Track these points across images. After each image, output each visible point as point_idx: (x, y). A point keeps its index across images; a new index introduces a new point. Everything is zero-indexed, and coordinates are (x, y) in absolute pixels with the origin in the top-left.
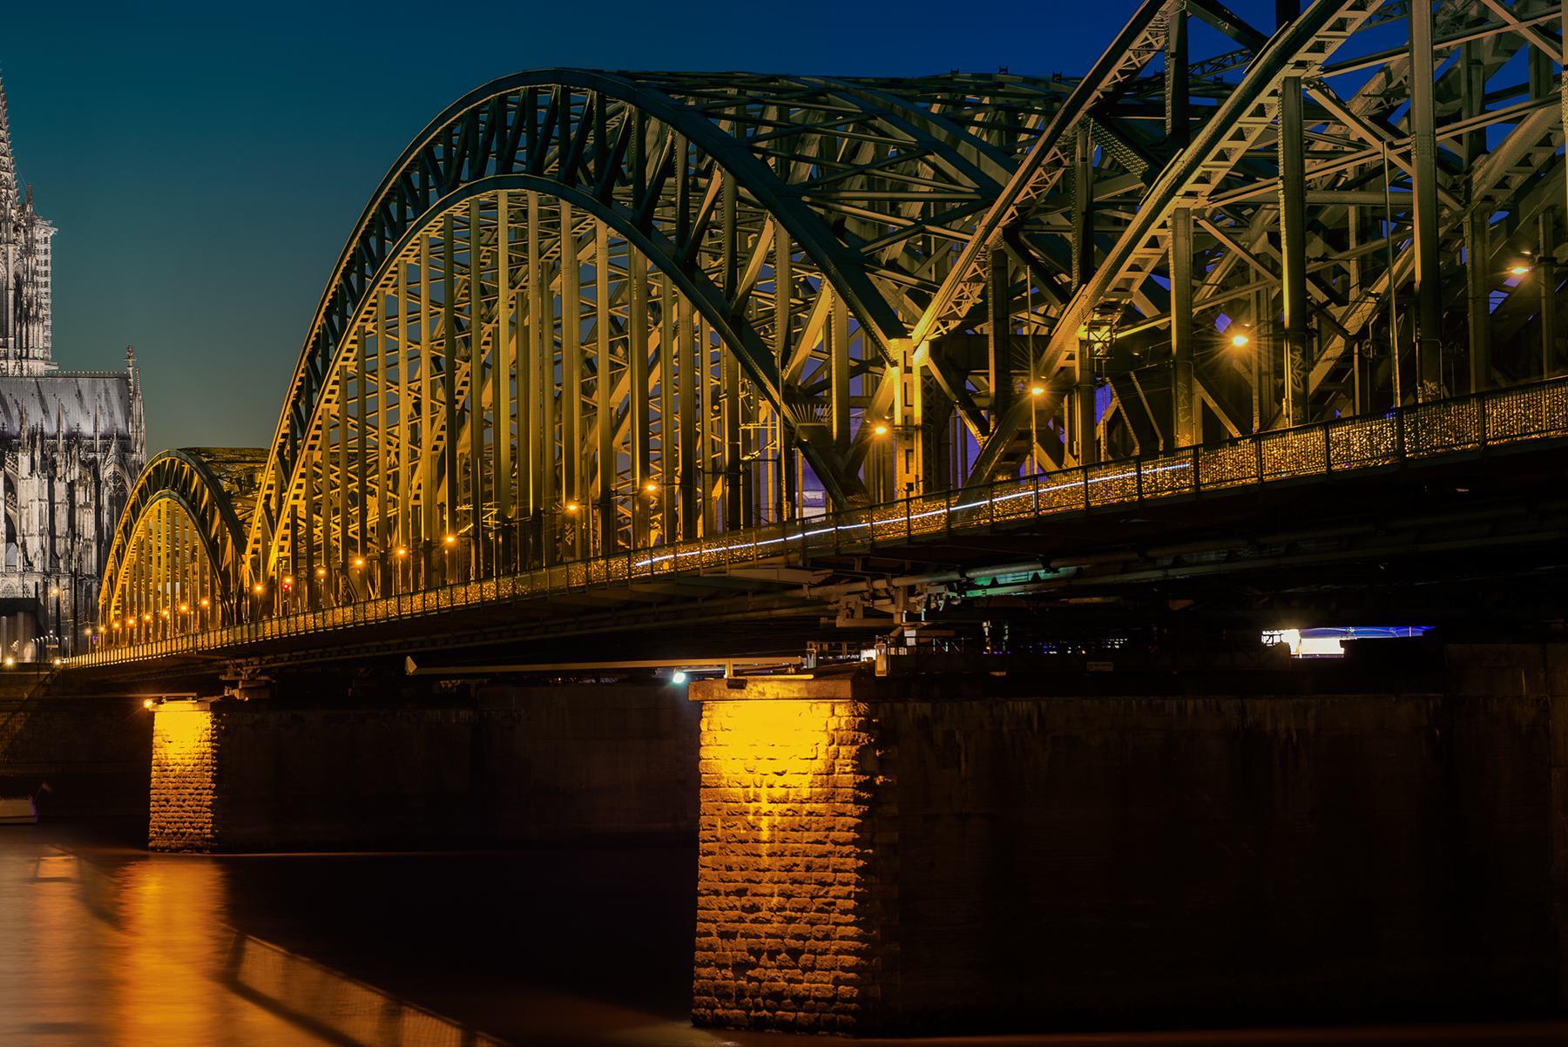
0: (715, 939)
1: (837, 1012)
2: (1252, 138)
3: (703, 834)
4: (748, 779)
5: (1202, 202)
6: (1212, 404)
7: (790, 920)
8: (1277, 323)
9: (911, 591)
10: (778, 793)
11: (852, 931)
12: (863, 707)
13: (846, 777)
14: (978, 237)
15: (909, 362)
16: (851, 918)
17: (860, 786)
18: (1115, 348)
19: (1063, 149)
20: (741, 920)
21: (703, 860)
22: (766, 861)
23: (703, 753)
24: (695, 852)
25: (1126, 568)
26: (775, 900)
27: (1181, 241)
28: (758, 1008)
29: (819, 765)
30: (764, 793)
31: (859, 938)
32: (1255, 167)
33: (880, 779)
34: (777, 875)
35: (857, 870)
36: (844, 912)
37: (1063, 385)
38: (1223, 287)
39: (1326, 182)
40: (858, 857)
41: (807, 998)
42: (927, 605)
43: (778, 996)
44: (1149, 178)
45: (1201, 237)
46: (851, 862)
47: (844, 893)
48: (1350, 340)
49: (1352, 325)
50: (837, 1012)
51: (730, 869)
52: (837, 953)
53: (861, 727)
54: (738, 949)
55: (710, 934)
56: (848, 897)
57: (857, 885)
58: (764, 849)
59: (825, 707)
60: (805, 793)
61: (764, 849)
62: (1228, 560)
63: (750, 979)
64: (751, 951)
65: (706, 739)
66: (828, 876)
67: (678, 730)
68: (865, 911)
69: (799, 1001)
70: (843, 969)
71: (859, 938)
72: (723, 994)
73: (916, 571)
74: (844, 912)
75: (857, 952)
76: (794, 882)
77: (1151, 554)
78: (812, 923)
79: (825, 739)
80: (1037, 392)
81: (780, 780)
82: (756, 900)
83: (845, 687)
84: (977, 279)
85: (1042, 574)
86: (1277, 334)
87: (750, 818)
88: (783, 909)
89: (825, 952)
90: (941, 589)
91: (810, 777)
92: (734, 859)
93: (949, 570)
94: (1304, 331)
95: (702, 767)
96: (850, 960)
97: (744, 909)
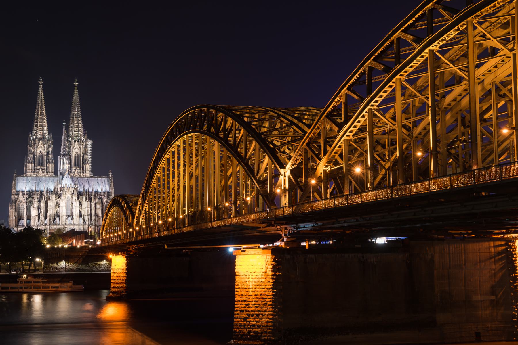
0: (239, 312)
1: (268, 329)
2: (362, 123)
3: (236, 287)
4: (246, 273)
5: (351, 137)
7: (257, 307)
8: (367, 166)
9: (286, 229)
10: (254, 277)
11: (271, 310)
12: (274, 256)
13: (270, 273)
14: (302, 144)
15: (286, 173)
16: (271, 306)
17: (273, 275)
18: (332, 171)
19: (320, 125)
20: (245, 307)
21: (236, 293)
22: (251, 293)
23: (236, 267)
24: (235, 291)
25: (334, 223)
26: (253, 303)
27: (346, 146)
28: (249, 328)
29: (264, 270)
31: (273, 311)
32: (362, 129)
33: (278, 273)
34: (254, 297)
35: (272, 295)
36: (269, 305)
37: (319, 179)
38: (358, 157)
39: (381, 133)
40: (273, 292)
41: (260, 326)
42: (289, 232)
43: (253, 325)
44: (339, 132)
45: (350, 145)
46: (271, 293)
48: (386, 170)
49: (387, 167)
50: (268, 329)
51: (242, 295)
52: (268, 315)
53: (273, 261)
54: (244, 315)
55: (237, 311)
56: (270, 302)
57: (272, 299)
58: (251, 290)
59: (265, 256)
60: (260, 277)
61: (251, 290)
62: (356, 221)
63: (247, 321)
64: (247, 315)
65: (237, 263)
66: (266, 297)
67: (230, 262)
68: (274, 305)
69: (259, 326)
70: (269, 319)
71: (273, 311)
72: (241, 325)
73: (286, 224)
74: (269, 305)
75: (272, 315)
76: (258, 298)
77: (339, 220)
78: (262, 308)
79: (265, 264)
80: (313, 182)
81: (254, 274)
82: (249, 303)
84: (300, 155)
85: (315, 224)
86: (367, 168)
87: (247, 283)
88: (255, 305)
89: (265, 315)
90: (292, 228)
91: (261, 273)
92: (243, 293)
93: (294, 224)
94: (374, 168)
95: (236, 270)
96: (271, 317)
97: (246, 305)
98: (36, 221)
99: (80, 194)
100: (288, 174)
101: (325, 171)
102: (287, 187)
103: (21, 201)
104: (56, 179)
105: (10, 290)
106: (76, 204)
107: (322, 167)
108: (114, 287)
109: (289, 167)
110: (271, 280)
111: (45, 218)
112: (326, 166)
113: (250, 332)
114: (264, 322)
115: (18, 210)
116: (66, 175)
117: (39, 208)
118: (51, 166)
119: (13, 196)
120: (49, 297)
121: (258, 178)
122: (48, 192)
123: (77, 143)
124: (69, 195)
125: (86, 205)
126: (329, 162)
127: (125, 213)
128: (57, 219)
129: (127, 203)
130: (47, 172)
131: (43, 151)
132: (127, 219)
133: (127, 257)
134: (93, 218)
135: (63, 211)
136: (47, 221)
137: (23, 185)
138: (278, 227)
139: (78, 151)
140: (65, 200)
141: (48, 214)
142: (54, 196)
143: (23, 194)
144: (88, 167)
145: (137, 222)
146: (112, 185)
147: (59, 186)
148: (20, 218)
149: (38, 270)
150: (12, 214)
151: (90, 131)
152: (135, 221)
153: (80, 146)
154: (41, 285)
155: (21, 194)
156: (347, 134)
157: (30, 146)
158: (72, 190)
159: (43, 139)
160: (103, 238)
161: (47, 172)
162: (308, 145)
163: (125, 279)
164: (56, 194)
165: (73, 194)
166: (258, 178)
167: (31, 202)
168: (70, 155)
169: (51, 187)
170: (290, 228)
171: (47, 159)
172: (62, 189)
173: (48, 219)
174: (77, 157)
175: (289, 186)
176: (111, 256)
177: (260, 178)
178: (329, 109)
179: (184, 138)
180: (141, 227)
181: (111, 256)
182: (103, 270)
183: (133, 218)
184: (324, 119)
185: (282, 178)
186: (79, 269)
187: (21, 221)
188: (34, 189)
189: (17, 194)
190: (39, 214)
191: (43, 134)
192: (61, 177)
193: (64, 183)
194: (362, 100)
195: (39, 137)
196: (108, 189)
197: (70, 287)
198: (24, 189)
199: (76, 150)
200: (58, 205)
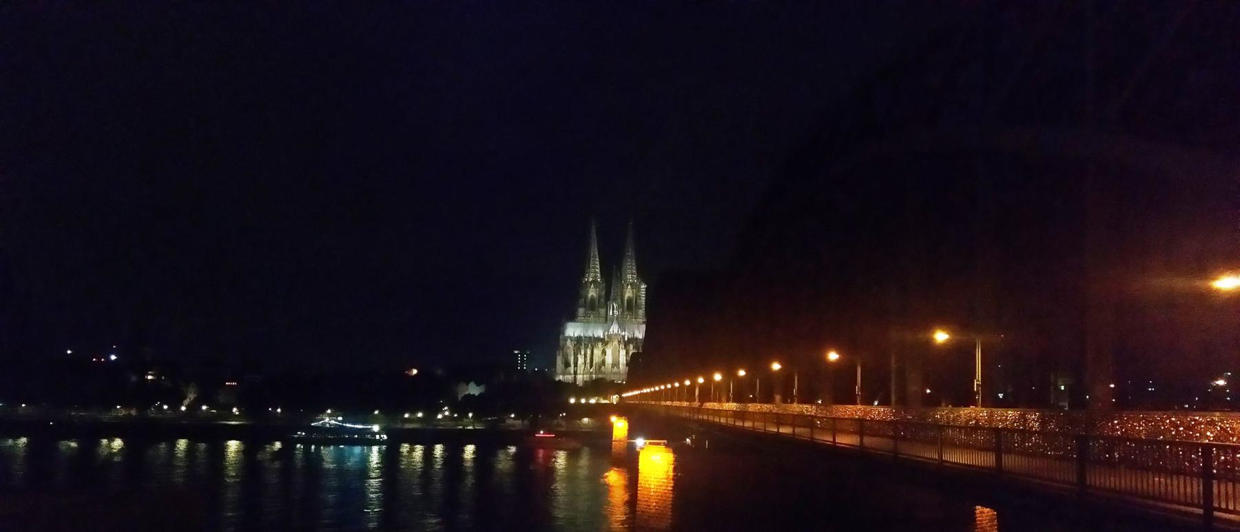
106: (623, 352)
119: (561, 343)
120: (573, 455)
122: (598, 339)
124: (616, 342)
135: (609, 360)
137: (573, 330)
142: (600, 344)
144: (641, 312)
148: (567, 365)
150: (559, 360)
151: (642, 274)
153: (633, 288)
159: (594, 282)
169: (599, 333)
172: (610, 336)
174: (630, 300)
176: (614, 419)
181: (614, 419)
189: (566, 339)
191: (596, 277)
199: (629, 293)
200: (604, 352)
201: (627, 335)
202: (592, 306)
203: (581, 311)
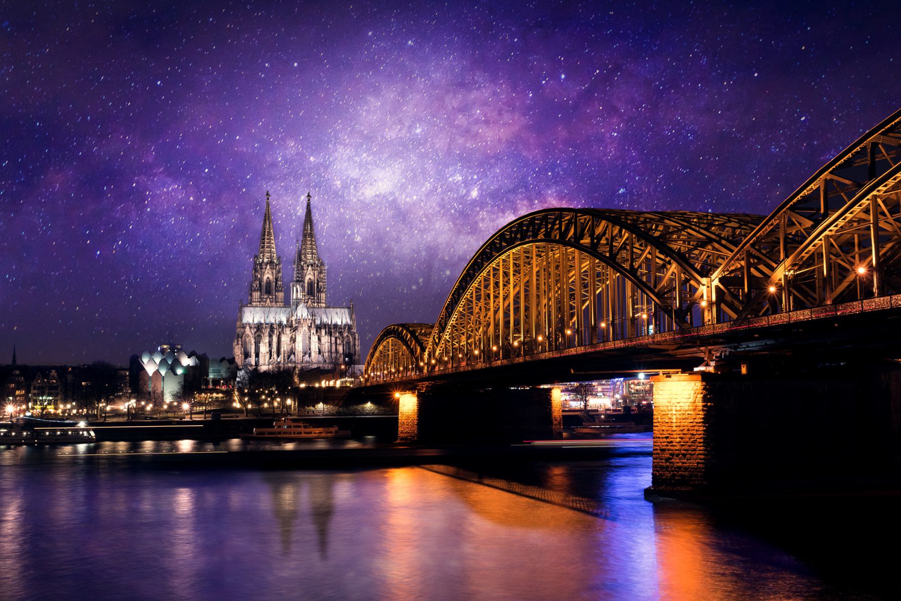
4: (668, 404)
6: (812, 293)
10: (678, 408)
13: (700, 404)
17: (704, 406)
22: (674, 428)
26: (678, 440)
29: (691, 400)
30: (674, 408)
43: (678, 467)
46: (701, 428)
47: (699, 438)
53: (704, 389)
54: (666, 455)
58: (674, 425)
59: (693, 383)
60: (687, 408)
61: (674, 425)
66: (695, 432)
69: (686, 469)
83: (700, 377)
92: (664, 428)
96: (702, 457)
98: (267, 359)
99: (319, 328)
100: (716, 282)
101: (786, 276)
102: (714, 299)
103: (249, 336)
104: (289, 310)
105: (266, 436)
106: (314, 339)
107: (781, 273)
108: (402, 432)
109: (716, 275)
110: (701, 412)
111: (278, 356)
112: (789, 271)
113: (674, 475)
114: (693, 463)
115: (244, 346)
116: (301, 306)
117: (270, 345)
118: (281, 295)
119: (239, 330)
121: (656, 291)
122: (280, 324)
123: (310, 268)
124: (306, 328)
125: (325, 339)
126: (793, 265)
127: (408, 347)
128: (292, 357)
129: (411, 332)
130: (276, 302)
131: (271, 277)
132: (412, 352)
133: (418, 396)
134: (334, 355)
135: (299, 347)
136: (281, 359)
138: (702, 348)
139: (312, 278)
140: (301, 335)
141: (282, 350)
142: (288, 331)
143: (251, 328)
145: (429, 355)
146: (354, 317)
147: (294, 318)
148: (247, 355)
149: (291, 415)
152: (426, 353)
154: (302, 429)
155: (248, 327)
156: (831, 228)
157: (256, 271)
158: (309, 322)
159: (271, 263)
160: (369, 376)
161: (276, 302)
162: (753, 245)
163: (416, 422)
164: (291, 326)
165: (310, 327)
166: (656, 291)
167: (259, 336)
168: (303, 281)
170: (718, 351)
171: (276, 286)
172: (298, 322)
173: (282, 356)
174: (311, 284)
175: (717, 297)
176: (397, 395)
177: (659, 291)
178: (795, 200)
179: (514, 250)
180: (440, 361)
181: (397, 395)
182: (368, 414)
183: (423, 349)
184: (785, 212)
185: (703, 290)
186: (338, 413)
187: (249, 359)
188: (263, 322)
190: (270, 351)
192: (294, 307)
193: (299, 315)
194: (861, 186)
195: (266, 260)
196: (349, 322)
197: (336, 432)
198: (251, 322)
200: (293, 340)
201: (318, 322)
202: (268, 290)
203: (256, 295)
